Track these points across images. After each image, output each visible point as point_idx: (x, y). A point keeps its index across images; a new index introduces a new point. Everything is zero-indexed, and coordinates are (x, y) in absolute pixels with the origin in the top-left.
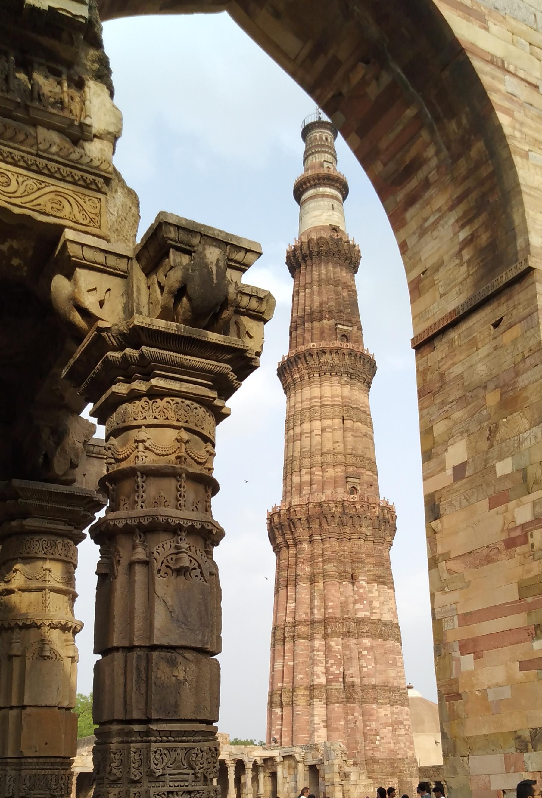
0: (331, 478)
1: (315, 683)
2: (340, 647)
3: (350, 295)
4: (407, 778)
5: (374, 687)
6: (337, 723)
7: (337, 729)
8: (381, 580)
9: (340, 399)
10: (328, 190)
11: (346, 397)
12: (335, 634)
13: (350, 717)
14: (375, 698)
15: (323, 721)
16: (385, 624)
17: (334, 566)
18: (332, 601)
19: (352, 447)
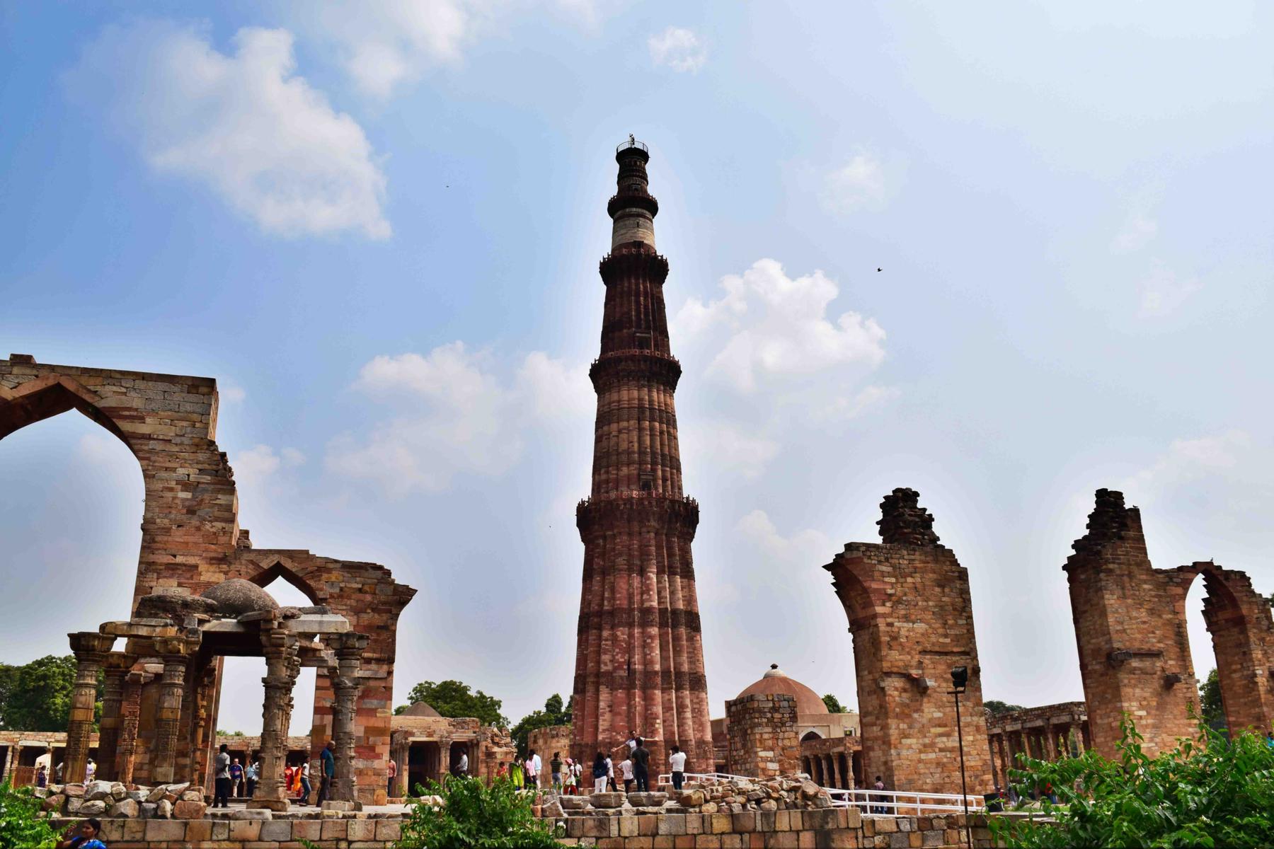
5: (656, 673)
7: (619, 714)
12: (621, 624)
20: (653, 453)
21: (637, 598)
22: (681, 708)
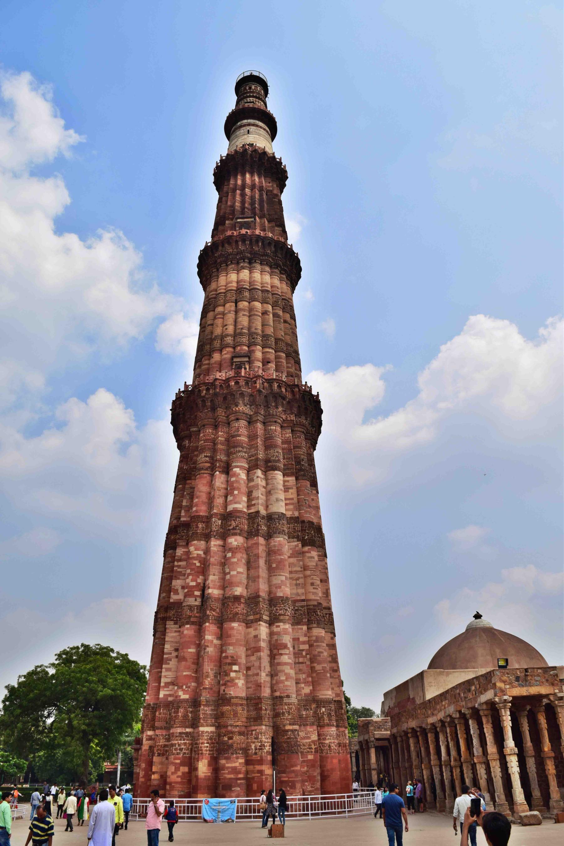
0: (215, 363)
1: (171, 601)
2: (201, 553)
3: (261, 195)
4: (284, 726)
5: (237, 599)
6: (185, 650)
7: (184, 659)
8: (269, 464)
9: (235, 284)
10: (246, 121)
11: (241, 281)
13: (203, 641)
14: (237, 614)
15: (177, 650)
16: (270, 518)
17: (206, 456)
18: (197, 498)
19: (241, 327)
20: (251, 334)
21: (219, 501)
22: (275, 649)
